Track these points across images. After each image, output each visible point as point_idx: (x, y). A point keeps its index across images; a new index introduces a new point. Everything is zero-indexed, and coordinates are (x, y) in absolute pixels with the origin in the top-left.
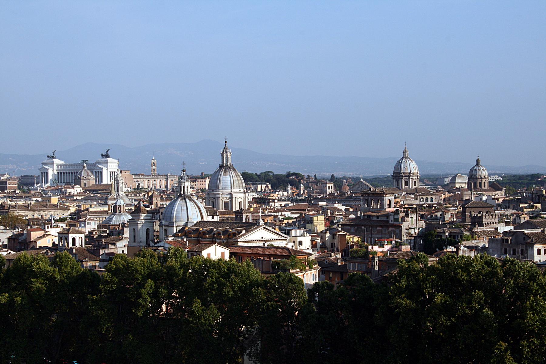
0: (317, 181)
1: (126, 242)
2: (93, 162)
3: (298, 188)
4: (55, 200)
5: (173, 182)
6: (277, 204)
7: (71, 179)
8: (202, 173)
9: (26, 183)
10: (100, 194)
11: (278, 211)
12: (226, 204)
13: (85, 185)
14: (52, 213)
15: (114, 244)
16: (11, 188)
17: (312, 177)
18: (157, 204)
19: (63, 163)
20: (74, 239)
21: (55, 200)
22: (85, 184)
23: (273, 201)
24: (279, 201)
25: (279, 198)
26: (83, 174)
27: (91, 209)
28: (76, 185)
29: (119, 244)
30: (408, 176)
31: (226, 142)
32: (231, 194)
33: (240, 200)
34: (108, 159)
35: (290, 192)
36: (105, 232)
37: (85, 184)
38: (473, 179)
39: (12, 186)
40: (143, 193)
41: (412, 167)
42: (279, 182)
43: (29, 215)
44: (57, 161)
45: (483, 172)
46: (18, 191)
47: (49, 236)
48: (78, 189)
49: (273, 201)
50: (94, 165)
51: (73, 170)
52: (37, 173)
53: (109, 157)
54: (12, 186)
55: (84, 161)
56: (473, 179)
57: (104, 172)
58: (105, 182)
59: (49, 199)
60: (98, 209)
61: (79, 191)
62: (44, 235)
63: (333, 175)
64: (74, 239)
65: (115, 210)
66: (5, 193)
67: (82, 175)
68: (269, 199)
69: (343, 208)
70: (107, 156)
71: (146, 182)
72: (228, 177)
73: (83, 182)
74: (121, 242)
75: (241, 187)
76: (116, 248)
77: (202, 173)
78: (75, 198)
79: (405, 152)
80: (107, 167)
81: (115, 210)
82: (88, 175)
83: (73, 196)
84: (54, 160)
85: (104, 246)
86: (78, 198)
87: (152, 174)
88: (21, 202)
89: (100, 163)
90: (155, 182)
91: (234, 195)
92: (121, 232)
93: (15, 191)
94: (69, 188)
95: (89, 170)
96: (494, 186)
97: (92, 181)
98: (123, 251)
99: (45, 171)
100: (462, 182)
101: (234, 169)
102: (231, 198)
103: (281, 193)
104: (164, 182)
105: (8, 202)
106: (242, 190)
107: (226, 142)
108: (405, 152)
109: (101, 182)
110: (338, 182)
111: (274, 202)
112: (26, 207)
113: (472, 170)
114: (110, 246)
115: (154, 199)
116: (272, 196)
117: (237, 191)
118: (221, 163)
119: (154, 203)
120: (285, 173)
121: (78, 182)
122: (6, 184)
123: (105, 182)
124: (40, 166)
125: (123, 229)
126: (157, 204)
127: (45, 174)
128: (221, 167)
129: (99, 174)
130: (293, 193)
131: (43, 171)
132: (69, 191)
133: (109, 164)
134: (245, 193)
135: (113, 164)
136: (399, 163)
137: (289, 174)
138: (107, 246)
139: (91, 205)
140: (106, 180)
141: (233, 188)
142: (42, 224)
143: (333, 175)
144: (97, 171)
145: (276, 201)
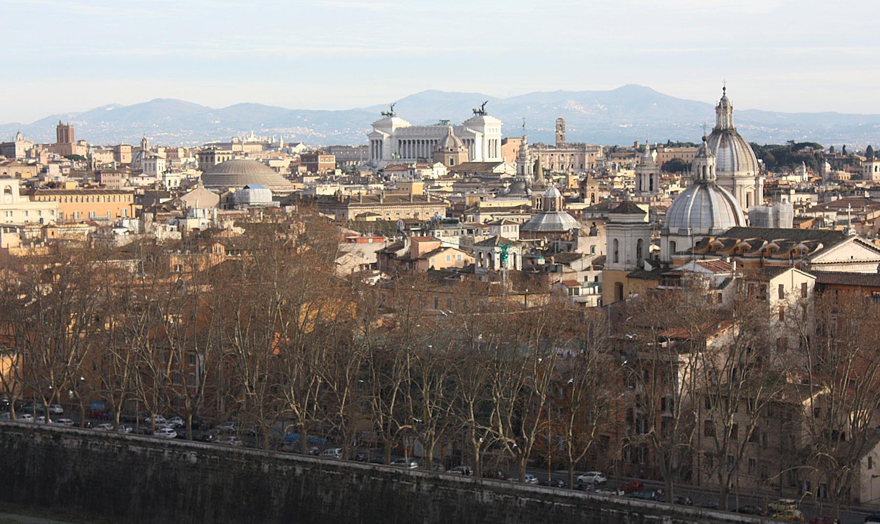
1: (587, 262)
2: (460, 123)
4: (418, 188)
7: (427, 151)
8: (636, 143)
13: (452, 164)
14: (418, 209)
15: (568, 265)
16: (324, 166)
18: (593, 196)
19: (408, 125)
22: (452, 161)
23: (787, 192)
24: (797, 191)
26: (448, 143)
27: (483, 205)
28: (435, 162)
29: (575, 265)
31: (724, 89)
33: (747, 190)
34: (484, 117)
35: (806, 176)
36: (539, 243)
37: (452, 161)
39: (326, 162)
40: (555, 178)
46: (338, 172)
47: (449, 250)
48: (439, 170)
49: (787, 192)
51: (426, 136)
53: (486, 114)
60: (495, 204)
61: (441, 174)
62: (440, 248)
63: (869, 147)
65: (548, 206)
66: (318, 175)
67: (446, 146)
68: (780, 189)
70: (482, 113)
71: (548, 157)
72: (728, 149)
74: (579, 261)
75: (751, 167)
76: (575, 272)
77: (636, 143)
78: (436, 185)
80: (483, 132)
81: (548, 206)
82: (455, 146)
83: (433, 180)
84: (393, 119)
85: (554, 269)
86: (441, 185)
90: (562, 159)
91: (738, 182)
92: (572, 244)
93: (333, 173)
94: (425, 168)
95: (459, 137)
97: (463, 157)
98: (586, 278)
99: (378, 139)
101: (738, 135)
103: (791, 178)
105: (345, 193)
106: (752, 173)
107: (724, 89)
111: (789, 194)
112: (375, 200)
114: (565, 269)
115: (588, 187)
117: (744, 174)
118: (714, 125)
119: (589, 194)
120: (782, 142)
122: (317, 160)
123: (478, 159)
124: (370, 130)
125: (575, 239)
126: (593, 196)
128: (716, 132)
129: (469, 142)
130: (809, 178)
131: (374, 139)
132: (426, 172)
133: (486, 127)
134: (757, 179)
138: (559, 268)
139: (482, 198)
141: (736, 169)
142: (428, 228)
143: (869, 147)
144: (466, 138)
145: (792, 192)
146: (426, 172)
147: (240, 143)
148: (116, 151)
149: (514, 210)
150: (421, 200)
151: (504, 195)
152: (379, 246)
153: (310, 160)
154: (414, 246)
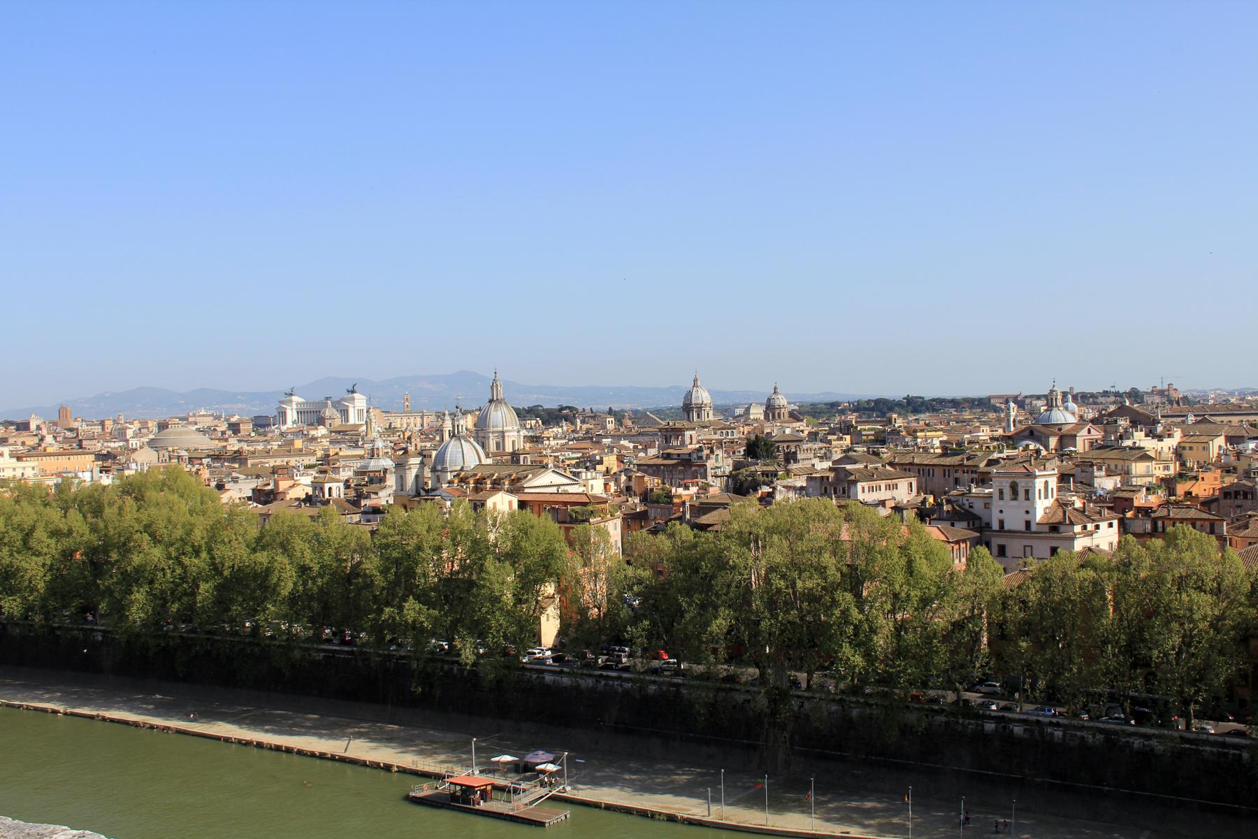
0: (594, 416)
3: (573, 423)
5: (429, 420)
6: (553, 443)
9: (261, 424)
10: (348, 436)
11: (557, 450)
12: (498, 444)
17: (588, 408)
20: (330, 489)
21: (298, 444)
23: (548, 439)
25: (555, 435)
30: (700, 408)
32: (503, 432)
38: (771, 410)
39: (246, 428)
41: (703, 396)
42: (552, 417)
43: (272, 462)
44: (295, 399)
45: (781, 401)
48: (322, 431)
49: (548, 439)
50: (339, 402)
52: (275, 413)
54: (246, 428)
55: (327, 399)
56: (771, 410)
57: (351, 411)
58: (351, 421)
59: (292, 443)
64: (330, 489)
69: (631, 445)
73: (328, 422)
79: (695, 380)
87: (407, 412)
88: (260, 447)
89: (345, 400)
92: (382, 480)
96: (794, 416)
97: (337, 422)
100: (757, 412)
102: (503, 437)
104: (419, 420)
105: (245, 447)
108: (695, 380)
109: (347, 420)
110: (619, 416)
113: (769, 400)
114: (373, 496)
116: (546, 434)
120: (555, 406)
121: (321, 421)
123: (351, 421)
127: (283, 414)
128: (491, 401)
129: (345, 413)
132: (312, 432)
135: (360, 401)
136: (690, 394)
137: (562, 409)
140: (353, 419)
142: (286, 471)
146: (312, 432)
147: (194, 415)
148: (102, 424)
149: (362, 457)
150: (300, 452)
151: (357, 446)
152: (254, 486)
153: (235, 428)
154: (276, 484)
